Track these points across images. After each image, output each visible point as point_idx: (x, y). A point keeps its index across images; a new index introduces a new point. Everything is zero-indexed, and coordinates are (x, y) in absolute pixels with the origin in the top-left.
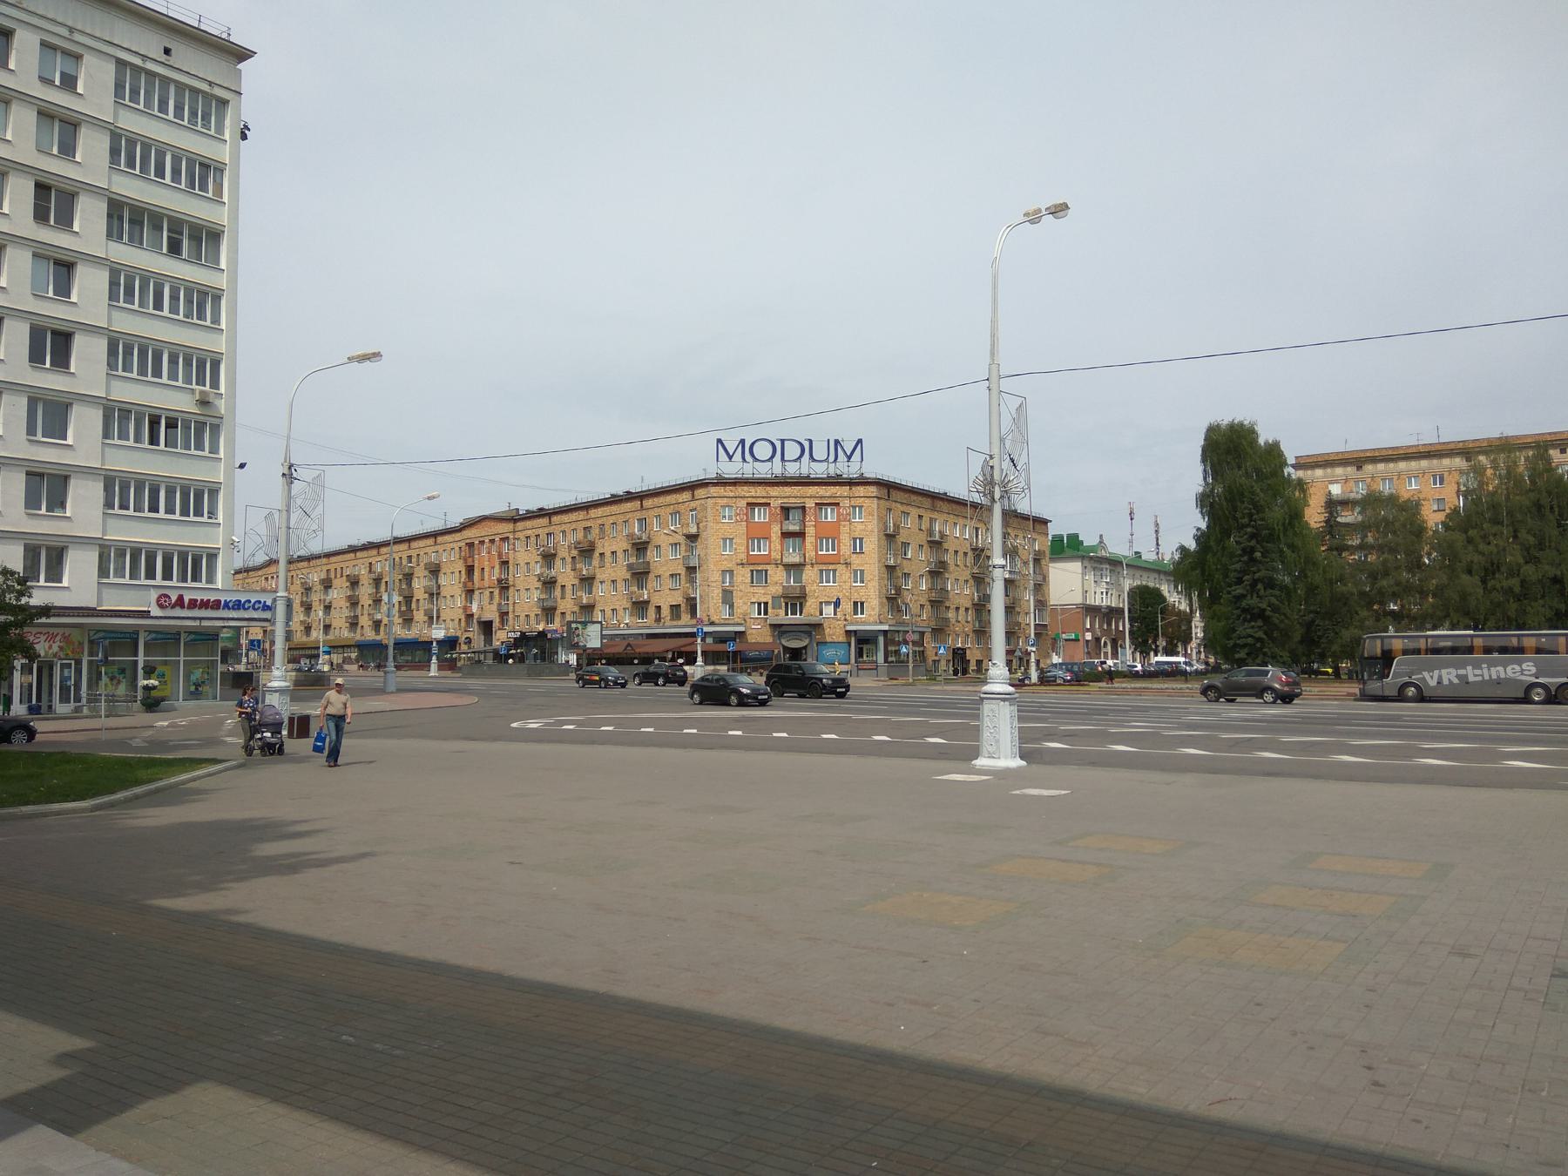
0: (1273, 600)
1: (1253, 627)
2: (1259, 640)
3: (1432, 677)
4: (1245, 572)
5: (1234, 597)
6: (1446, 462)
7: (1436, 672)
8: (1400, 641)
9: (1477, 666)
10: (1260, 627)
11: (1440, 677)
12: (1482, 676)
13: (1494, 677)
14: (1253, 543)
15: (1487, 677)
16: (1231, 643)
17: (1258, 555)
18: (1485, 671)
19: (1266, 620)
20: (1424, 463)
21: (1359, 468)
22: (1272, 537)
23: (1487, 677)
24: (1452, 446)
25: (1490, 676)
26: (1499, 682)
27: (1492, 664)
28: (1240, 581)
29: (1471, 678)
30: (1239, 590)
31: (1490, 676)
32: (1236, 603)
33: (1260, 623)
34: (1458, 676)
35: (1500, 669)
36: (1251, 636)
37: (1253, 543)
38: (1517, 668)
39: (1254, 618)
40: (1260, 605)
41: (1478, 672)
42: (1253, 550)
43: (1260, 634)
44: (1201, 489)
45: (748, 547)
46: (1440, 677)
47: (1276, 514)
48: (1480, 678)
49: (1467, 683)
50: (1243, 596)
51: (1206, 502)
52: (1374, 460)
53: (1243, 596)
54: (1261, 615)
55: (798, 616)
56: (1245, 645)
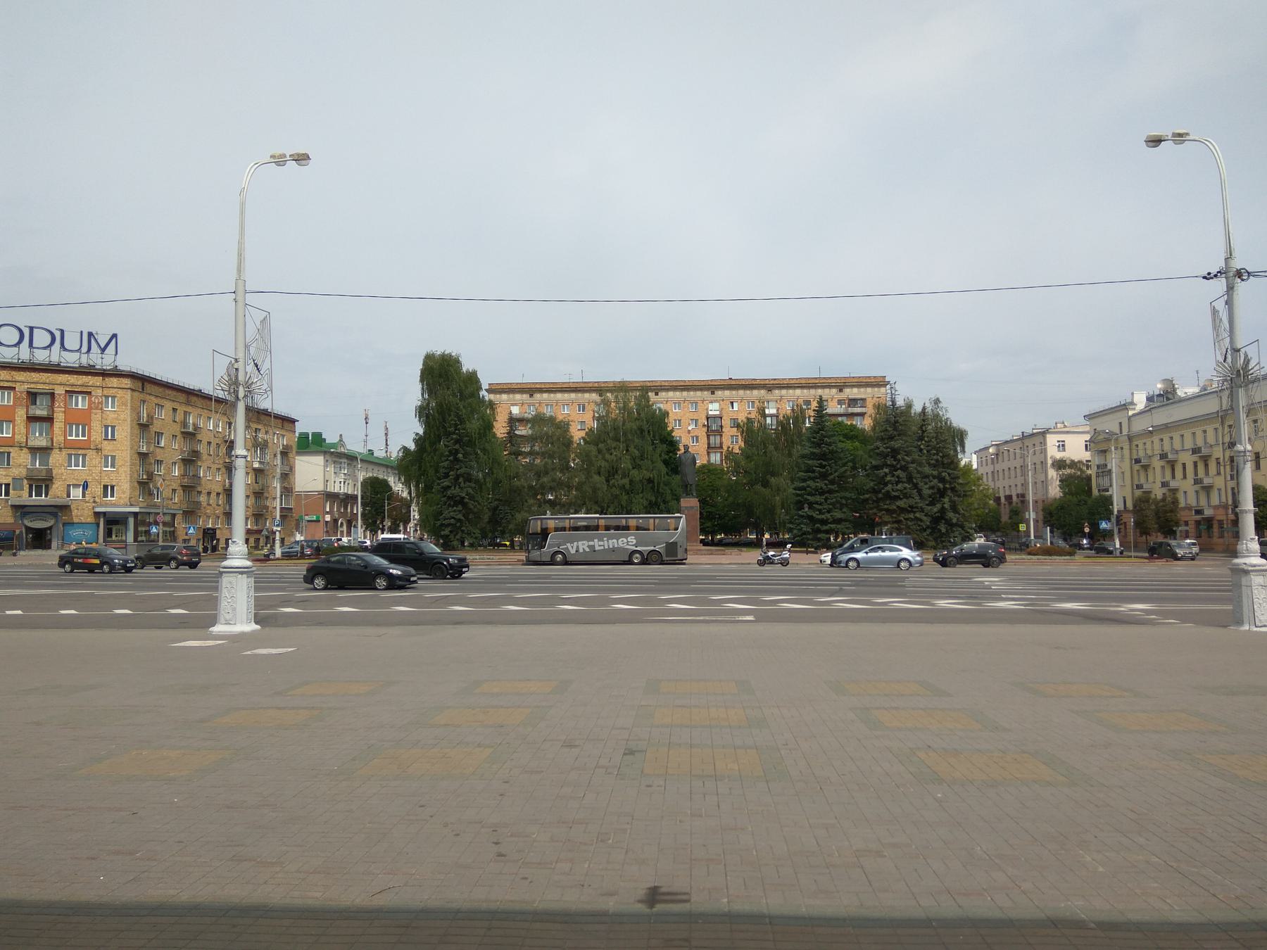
0: (470, 491)
1: (454, 511)
2: (459, 520)
3: (572, 547)
4: (451, 469)
5: (443, 487)
6: (587, 395)
7: (575, 543)
8: (553, 521)
9: (601, 539)
10: (460, 511)
11: (578, 547)
12: (604, 546)
13: (611, 547)
14: (457, 446)
15: (606, 547)
16: (438, 523)
17: (460, 456)
18: (606, 542)
19: (464, 505)
20: (573, 395)
21: (531, 396)
22: (471, 443)
23: (606, 547)
24: (590, 385)
25: (609, 546)
26: (613, 550)
27: (610, 538)
28: (446, 476)
29: (597, 548)
30: (446, 483)
31: (609, 546)
32: (443, 492)
33: (460, 508)
34: (588, 546)
35: (615, 541)
36: (453, 518)
37: (457, 446)
38: (625, 540)
39: (456, 504)
40: (460, 494)
41: (601, 543)
42: (457, 452)
43: (460, 516)
44: (419, 403)
45: (65, 431)
46: (578, 547)
47: (473, 425)
48: (602, 548)
49: (595, 551)
50: (449, 487)
51: (423, 412)
52: (541, 391)
53: (449, 487)
54: (461, 502)
55: (109, 498)
56: (449, 525)
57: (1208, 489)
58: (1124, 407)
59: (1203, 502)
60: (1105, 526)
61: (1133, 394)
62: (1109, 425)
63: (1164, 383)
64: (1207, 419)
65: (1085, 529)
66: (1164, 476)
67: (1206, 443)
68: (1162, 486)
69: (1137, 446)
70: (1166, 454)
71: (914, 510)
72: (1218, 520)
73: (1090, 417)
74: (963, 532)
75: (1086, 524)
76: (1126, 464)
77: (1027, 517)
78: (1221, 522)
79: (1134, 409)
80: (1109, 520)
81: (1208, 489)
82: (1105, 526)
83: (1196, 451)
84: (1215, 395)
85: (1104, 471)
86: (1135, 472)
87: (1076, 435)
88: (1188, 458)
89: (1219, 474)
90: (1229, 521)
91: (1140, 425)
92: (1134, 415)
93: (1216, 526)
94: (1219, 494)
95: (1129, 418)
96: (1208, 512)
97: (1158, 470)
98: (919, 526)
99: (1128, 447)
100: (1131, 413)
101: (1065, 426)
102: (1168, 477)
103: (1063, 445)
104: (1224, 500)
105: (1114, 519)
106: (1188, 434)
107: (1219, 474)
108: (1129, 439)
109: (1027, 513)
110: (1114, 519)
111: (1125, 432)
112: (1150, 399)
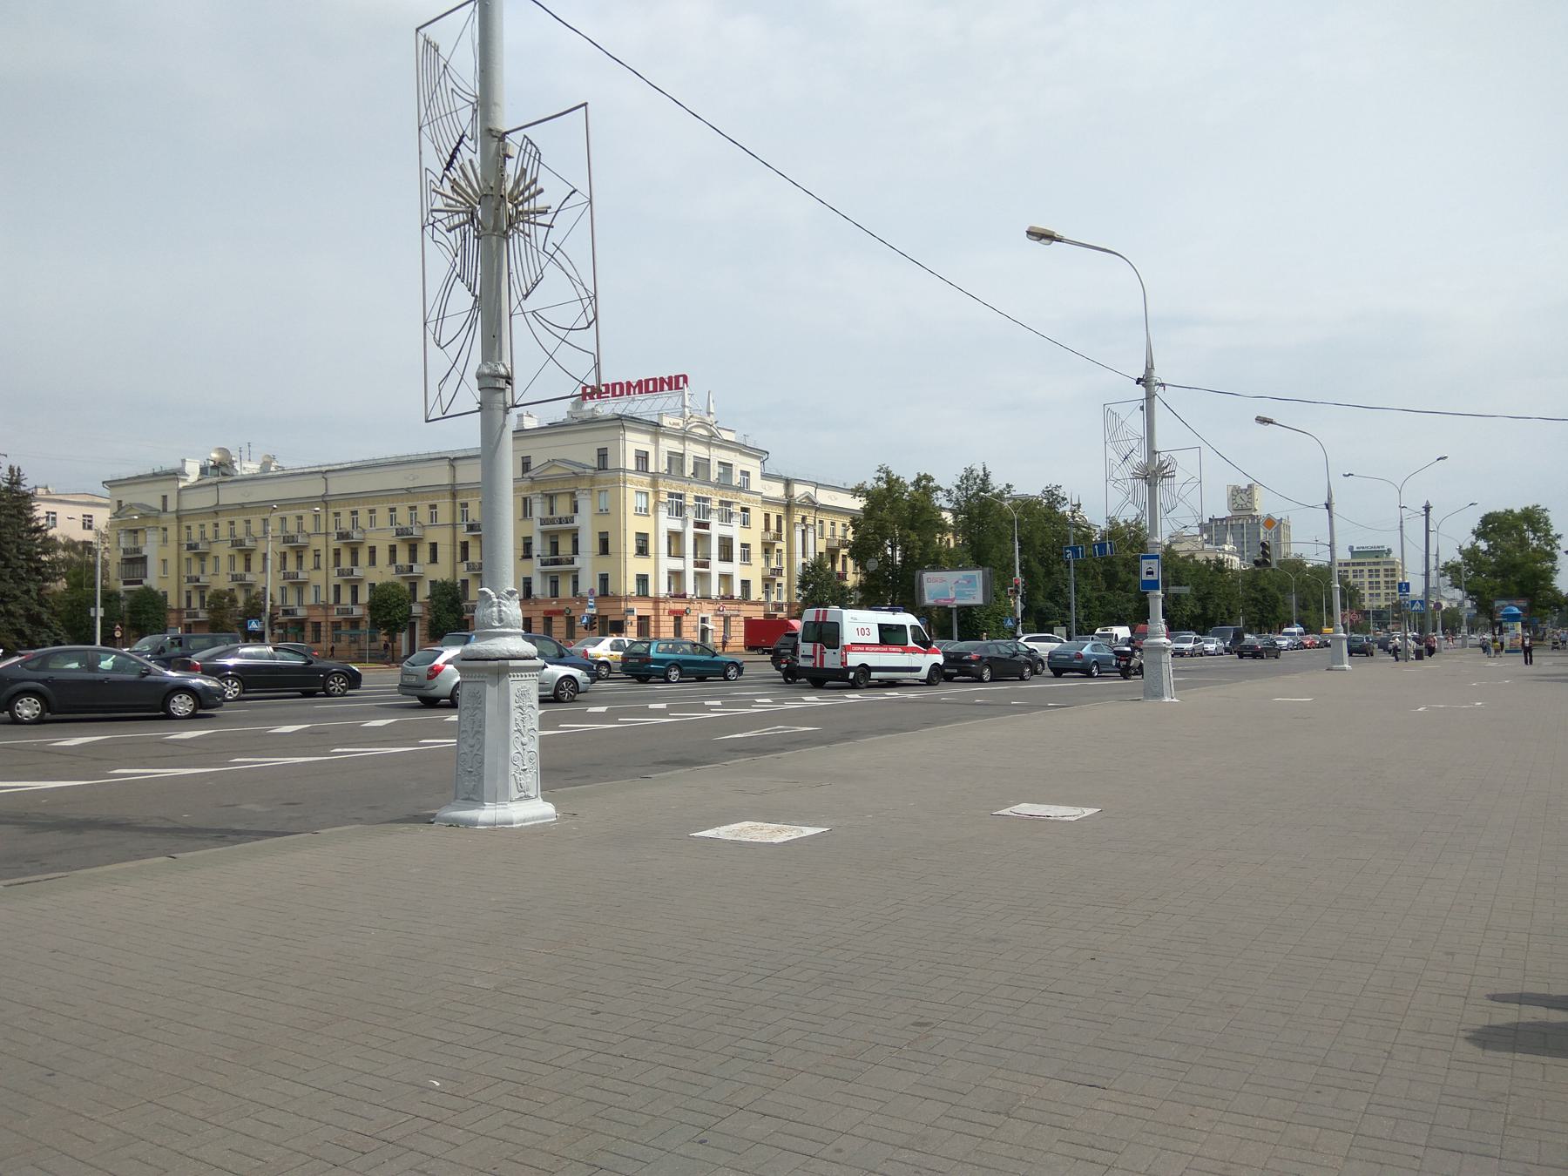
57: (300, 586)
58: (175, 475)
59: (292, 601)
60: (255, 626)
61: (184, 461)
62: (150, 497)
63: (219, 453)
64: (308, 502)
65: (116, 632)
66: (189, 570)
67: (248, 532)
68: (233, 580)
69: (189, 528)
70: (197, 545)
71: (6, 599)
72: (312, 623)
73: (111, 484)
74: (52, 634)
75: (118, 626)
76: (171, 552)
77: (92, 614)
78: (317, 625)
79: (185, 480)
80: (259, 618)
81: (300, 586)
82: (255, 626)
83: (342, 536)
84: (320, 476)
85: (135, 561)
86: (184, 562)
87: (71, 506)
88: (223, 550)
89: (317, 567)
90: (329, 624)
91: (193, 502)
92: (185, 488)
93: (309, 628)
94: (316, 592)
95: (180, 491)
96: (301, 613)
97: (224, 563)
98: (10, 624)
99: (175, 528)
100: (181, 485)
101: (48, 493)
102: (240, 568)
103: (54, 519)
104: (323, 597)
105: (266, 619)
106: (223, 522)
107: (317, 567)
108: (178, 518)
109: (92, 610)
110: (266, 619)
111: (172, 506)
112: (203, 471)
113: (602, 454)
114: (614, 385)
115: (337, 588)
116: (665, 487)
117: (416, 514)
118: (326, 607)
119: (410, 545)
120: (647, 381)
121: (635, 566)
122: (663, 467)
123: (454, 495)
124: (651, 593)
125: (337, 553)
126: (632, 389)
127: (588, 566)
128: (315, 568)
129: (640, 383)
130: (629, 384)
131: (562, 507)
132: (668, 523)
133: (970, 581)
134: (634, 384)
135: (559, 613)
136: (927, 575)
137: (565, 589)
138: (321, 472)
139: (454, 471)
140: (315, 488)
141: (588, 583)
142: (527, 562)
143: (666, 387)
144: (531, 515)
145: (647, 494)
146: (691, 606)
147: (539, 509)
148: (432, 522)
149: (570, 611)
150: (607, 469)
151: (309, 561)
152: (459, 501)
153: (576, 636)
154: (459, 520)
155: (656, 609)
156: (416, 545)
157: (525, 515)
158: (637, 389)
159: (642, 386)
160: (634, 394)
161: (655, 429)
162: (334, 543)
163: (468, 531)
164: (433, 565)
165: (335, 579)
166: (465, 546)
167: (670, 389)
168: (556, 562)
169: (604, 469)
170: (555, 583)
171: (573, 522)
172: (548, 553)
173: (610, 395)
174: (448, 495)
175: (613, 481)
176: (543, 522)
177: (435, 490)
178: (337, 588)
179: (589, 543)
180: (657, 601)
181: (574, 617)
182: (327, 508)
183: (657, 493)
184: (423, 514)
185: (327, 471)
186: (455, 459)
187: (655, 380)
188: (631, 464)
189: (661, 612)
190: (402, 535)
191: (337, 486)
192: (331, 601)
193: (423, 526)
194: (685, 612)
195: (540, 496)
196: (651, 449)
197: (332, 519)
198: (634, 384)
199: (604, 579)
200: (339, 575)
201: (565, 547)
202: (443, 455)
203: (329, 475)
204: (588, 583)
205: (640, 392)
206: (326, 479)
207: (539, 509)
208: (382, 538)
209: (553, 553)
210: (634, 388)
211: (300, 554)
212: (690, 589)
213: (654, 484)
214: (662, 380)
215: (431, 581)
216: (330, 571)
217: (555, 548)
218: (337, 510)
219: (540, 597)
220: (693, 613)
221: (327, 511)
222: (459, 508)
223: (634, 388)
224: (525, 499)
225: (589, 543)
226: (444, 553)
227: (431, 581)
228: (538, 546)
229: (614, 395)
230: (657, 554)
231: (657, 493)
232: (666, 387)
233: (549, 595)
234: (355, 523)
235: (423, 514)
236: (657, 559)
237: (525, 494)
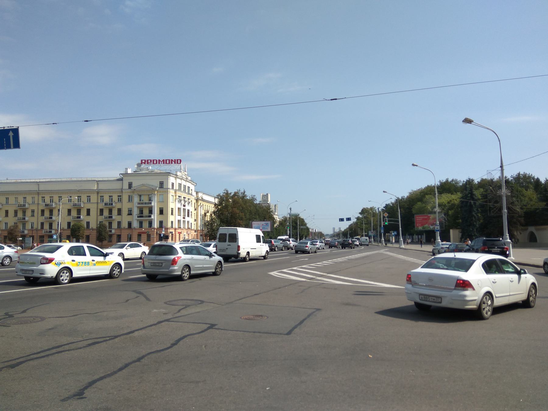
64: (30, 192)
89: (33, 216)
90: (38, 236)
104: (35, 227)
113: (162, 184)
114: (154, 160)
115: (42, 224)
116: (179, 193)
117: (90, 199)
118: (37, 230)
119: (78, 209)
120: (166, 160)
121: (171, 218)
122: (177, 189)
123: (98, 193)
124: (174, 227)
125: (43, 211)
126: (160, 162)
127: (155, 218)
128: (31, 216)
129: (163, 160)
130: (159, 160)
131: (145, 199)
132: (178, 205)
133: (267, 224)
134: (161, 161)
135: (144, 233)
136: (253, 222)
137: (146, 225)
138: (37, 182)
139: (98, 185)
140: (35, 188)
141: (156, 225)
142: (130, 216)
143: (173, 162)
144: (132, 201)
145: (173, 196)
146: (183, 231)
147: (136, 199)
148: (88, 201)
149: (149, 232)
150: (163, 188)
151: (29, 213)
152: (100, 195)
153: (151, 240)
154: (99, 201)
155: (175, 232)
156: (80, 209)
157: (129, 201)
158: (162, 162)
159: (165, 162)
160: (161, 164)
161: (176, 177)
162: (41, 208)
163: (105, 205)
164: (88, 217)
165: (42, 219)
166: (102, 211)
167: (175, 163)
168: (142, 217)
169: (162, 188)
170: (141, 223)
171: (151, 204)
172: (148, 214)
173: (152, 163)
174: (96, 193)
175: (165, 192)
176: (139, 204)
177: (92, 191)
178: (42, 224)
179: (156, 211)
180: (175, 229)
181: (150, 234)
182: (38, 195)
183: (176, 196)
184: (84, 198)
185: (39, 182)
186: (99, 181)
187: (169, 160)
188: (171, 188)
189: (176, 232)
190: (76, 206)
191: (42, 188)
192: (39, 228)
193: (84, 203)
194: (181, 233)
195: (137, 195)
196: (174, 182)
197: (40, 199)
198: (161, 161)
199: (161, 223)
200: (45, 219)
201: (146, 212)
202: (93, 179)
203: (39, 183)
204: (156, 225)
205: (164, 163)
206: (39, 185)
207: (136, 199)
208: (63, 207)
209: (141, 213)
210: (161, 162)
211: (24, 211)
212: (182, 227)
213: (175, 192)
214: (172, 160)
215: (87, 222)
216: (39, 218)
217: (141, 212)
218: (43, 196)
219: (137, 228)
220: (182, 233)
221: (38, 196)
222: (99, 198)
223: (161, 162)
224: (129, 196)
225: (156, 211)
226: (93, 212)
227: (87, 222)
228: (136, 212)
229: (153, 163)
230: (175, 215)
231: (176, 196)
232: (173, 162)
233: (148, 227)
234: (52, 201)
235: (84, 198)
236: (175, 216)
237: (129, 194)
